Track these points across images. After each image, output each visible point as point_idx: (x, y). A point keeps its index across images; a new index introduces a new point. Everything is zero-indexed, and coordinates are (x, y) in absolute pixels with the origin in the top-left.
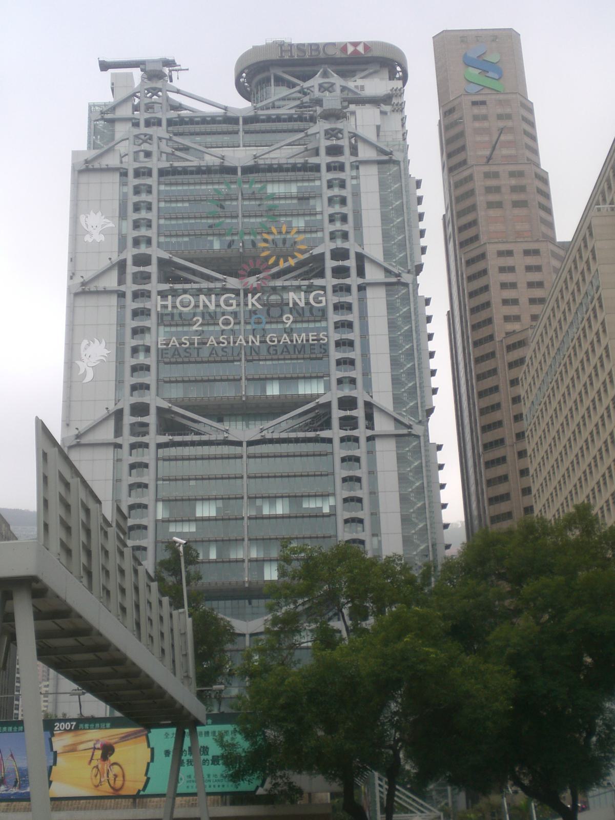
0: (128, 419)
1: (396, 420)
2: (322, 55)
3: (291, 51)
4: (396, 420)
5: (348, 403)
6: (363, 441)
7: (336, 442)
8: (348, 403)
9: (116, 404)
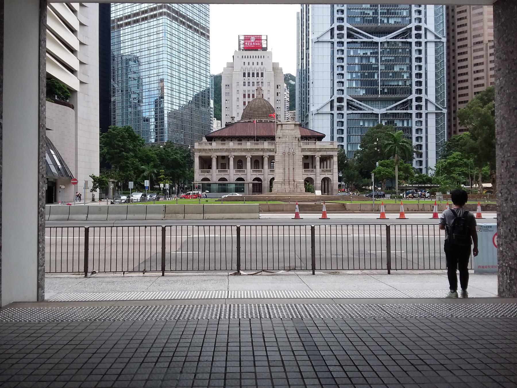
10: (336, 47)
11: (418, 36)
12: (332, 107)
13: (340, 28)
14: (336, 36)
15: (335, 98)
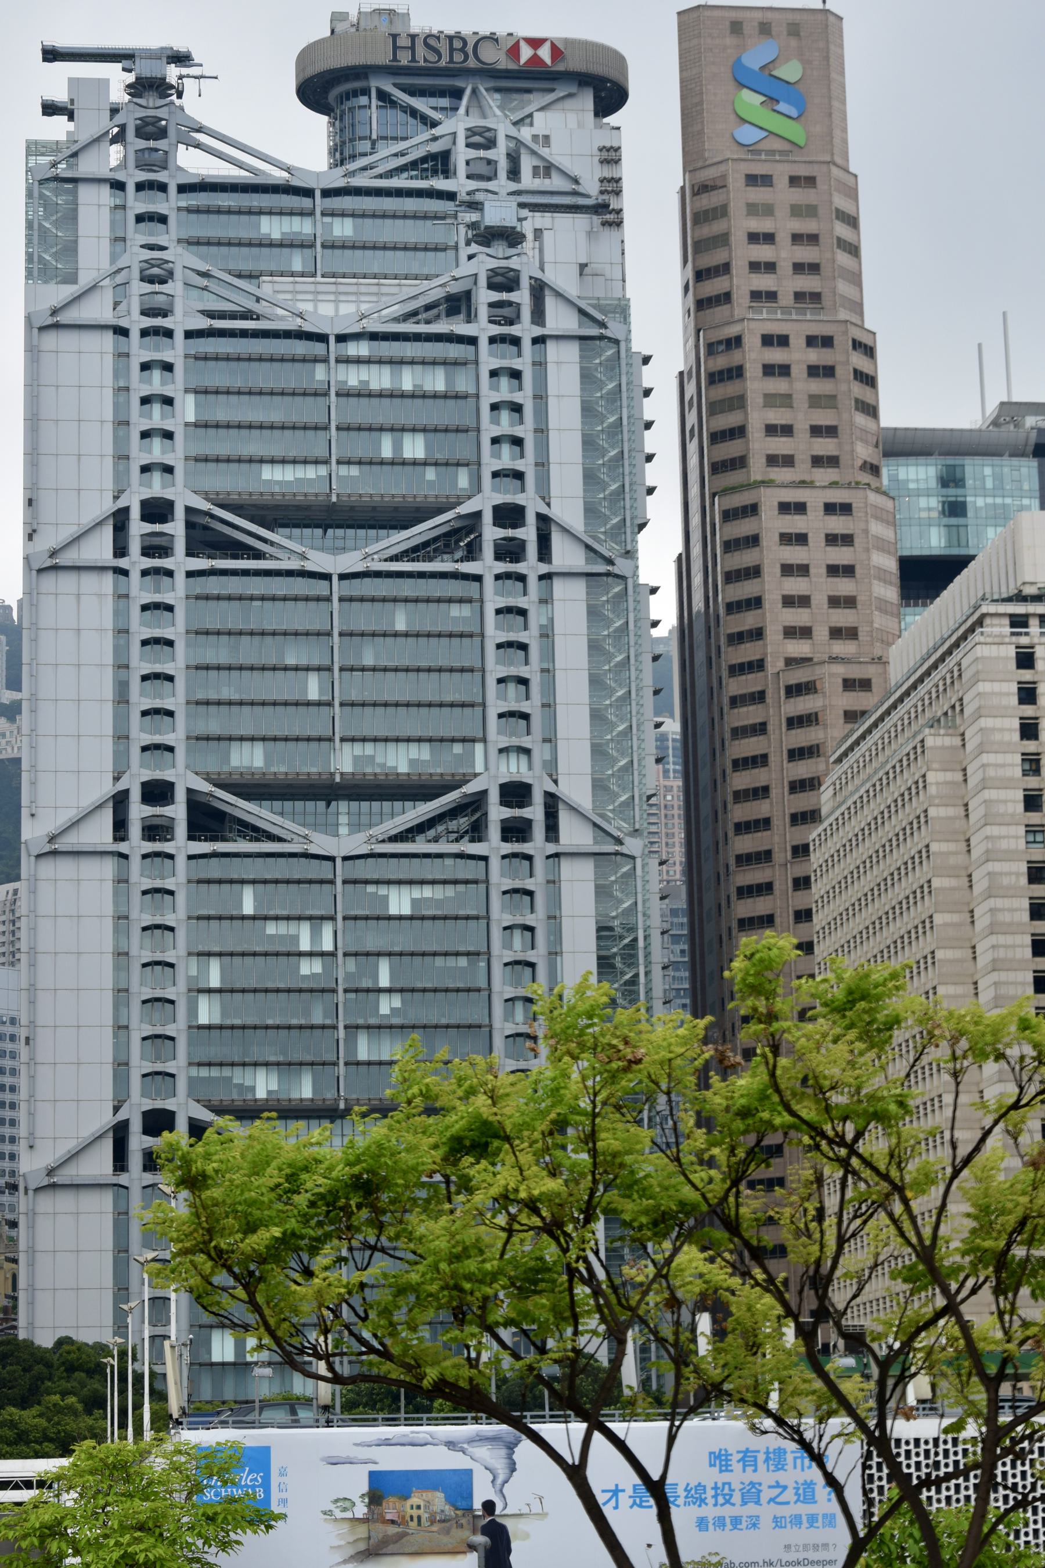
0: (138, 528)
1: (588, 547)
2: (472, 63)
3: (413, 48)
4: (588, 547)
5: (509, 515)
6: (532, 582)
7: (489, 582)
8: (509, 515)
9: (116, 498)
10: (140, 878)
11: (516, 831)
12: (120, 1161)
13: (157, 792)
14: (135, 830)
15: (133, 1114)
